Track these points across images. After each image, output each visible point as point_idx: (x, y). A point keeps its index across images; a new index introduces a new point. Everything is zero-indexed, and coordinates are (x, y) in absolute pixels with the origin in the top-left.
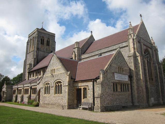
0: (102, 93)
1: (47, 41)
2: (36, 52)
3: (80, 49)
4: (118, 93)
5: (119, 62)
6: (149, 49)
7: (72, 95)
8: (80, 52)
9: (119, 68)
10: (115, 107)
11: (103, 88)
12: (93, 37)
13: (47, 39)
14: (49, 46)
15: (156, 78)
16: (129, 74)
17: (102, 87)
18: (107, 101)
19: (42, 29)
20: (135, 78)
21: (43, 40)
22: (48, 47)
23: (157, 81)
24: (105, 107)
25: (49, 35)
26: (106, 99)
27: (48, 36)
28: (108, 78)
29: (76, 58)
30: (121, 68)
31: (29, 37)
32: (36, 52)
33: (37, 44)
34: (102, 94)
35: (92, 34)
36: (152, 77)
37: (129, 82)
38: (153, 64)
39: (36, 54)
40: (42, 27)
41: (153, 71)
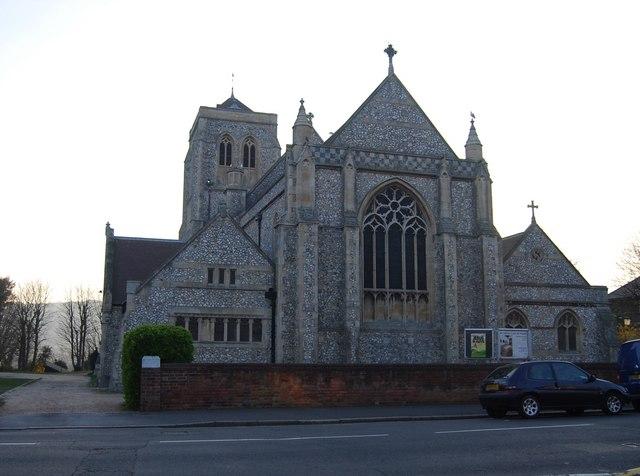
1: (246, 147)
6: (419, 184)
9: (211, 272)
14: (253, 165)
15: (441, 290)
16: (266, 288)
19: (232, 104)
20: (281, 300)
21: (229, 145)
23: (442, 303)
30: (222, 272)
32: (201, 196)
36: (423, 286)
37: (263, 312)
39: (199, 206)
40: (232, 95)
41: (431, 266)
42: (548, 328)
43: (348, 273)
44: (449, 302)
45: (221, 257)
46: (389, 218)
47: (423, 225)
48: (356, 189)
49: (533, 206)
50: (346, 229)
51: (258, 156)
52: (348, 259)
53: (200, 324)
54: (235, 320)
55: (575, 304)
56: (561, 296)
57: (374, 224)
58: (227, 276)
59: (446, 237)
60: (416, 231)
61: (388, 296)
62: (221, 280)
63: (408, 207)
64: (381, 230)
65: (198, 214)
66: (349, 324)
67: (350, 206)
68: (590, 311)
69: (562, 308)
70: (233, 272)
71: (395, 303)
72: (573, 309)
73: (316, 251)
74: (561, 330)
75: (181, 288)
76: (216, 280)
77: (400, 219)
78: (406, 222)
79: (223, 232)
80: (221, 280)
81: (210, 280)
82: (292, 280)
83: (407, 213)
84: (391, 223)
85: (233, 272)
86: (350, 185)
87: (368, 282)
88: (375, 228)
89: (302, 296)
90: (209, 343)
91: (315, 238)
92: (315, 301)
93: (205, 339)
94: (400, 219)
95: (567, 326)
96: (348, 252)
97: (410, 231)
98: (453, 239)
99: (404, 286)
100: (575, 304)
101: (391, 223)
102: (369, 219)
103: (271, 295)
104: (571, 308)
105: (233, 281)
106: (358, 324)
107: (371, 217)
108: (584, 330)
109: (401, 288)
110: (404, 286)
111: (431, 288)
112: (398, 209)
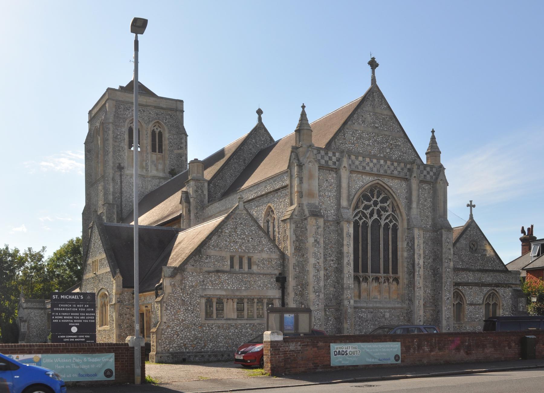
0: (165, 323)
1: (153, 133)
2: (111, 181)
3: (206, 185)
4: (223, 322)
5: (237, 242)
7: (127, 327)
8: (206, 192)
9: (232, 258)
10: (209, 353)
11: (167, 309)
12: (266, 130)
13: (151, 125)
14: (161, 151)
15: (410, 275)
16: (277, 272)
17: (164, 308)
18: (181, 339)
20: (291, 283)
22: (154, 156)
23: (411, 284)
24: (172, 353)
25: (156, 107)
26: (176, 336)
27: (157, 114)
28: (185, 287)
29: (190, 216)
30: (241, 259)
31: (91, 121)
33: (114, 152)
34: (163, 324)
35: (260, 119)
38: (408, 229)
41: (403, 254)
42: (479, 304)
43: (346, 261)
44: (417, 284)
45: (240, 246)
46: (371, 214)
47: (396, 220)
48: (349, 186)
49: (471, 206)
50: (342, 223)
51: (166, 142)
52: (345, 249)
53: (225, 304)
54: (253, 299)
55: (497, 285)
56: (488, 278)
57: (360, 219)
58: (245, 262)
59: (416, 232)
60: (391, 225)
61: (370, 279)
62: (241, 266)
63: (386, 205)
64: (365, 223)
65: (111, 197)
66: (346, 303)
67: (344, 203)
68: (507, 290)
69: (489, 288)
70: (249, 259)
71: (375, 284)
72: (497, 289)
73: (322, 241)
74: (488, 305)
75: (209, 272)
76: (237, 267)
77: (380, 215)
78: (383, 217)
79: (241, 224)
80: (241, 266)
81: (232, 266)
82: (302, 267)
83: (385, 209)
84: (373, 218)
85: (249, 259)
86: (344, 184)
87: (356, 269)
88: (361, 222)
89: (311, 278)
90: (233, 319)
91: (321, 230)
92: (322, 284)
93: (229, 317)
94: (380, 215)
95: (491, 303)
96: (345, 242)
97: (387, 225)
98: (421, 232)
99: (382, 270)
100: (497, 285)
101: (373, 218)
102: (356, 215)
103: (282, 280)
104: (495, 288)
105: (250, 267)
106: (352, 302)
107: (359, 212)
108: (503, 305)
109: (379, 273)
110: (382, 270)
111: (402, 273)
112: (378, 207)
